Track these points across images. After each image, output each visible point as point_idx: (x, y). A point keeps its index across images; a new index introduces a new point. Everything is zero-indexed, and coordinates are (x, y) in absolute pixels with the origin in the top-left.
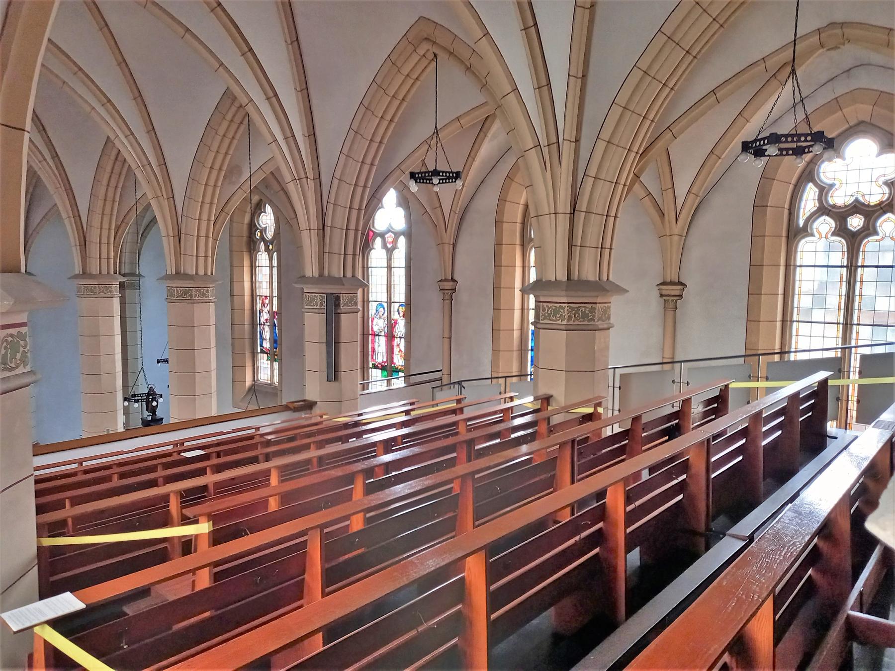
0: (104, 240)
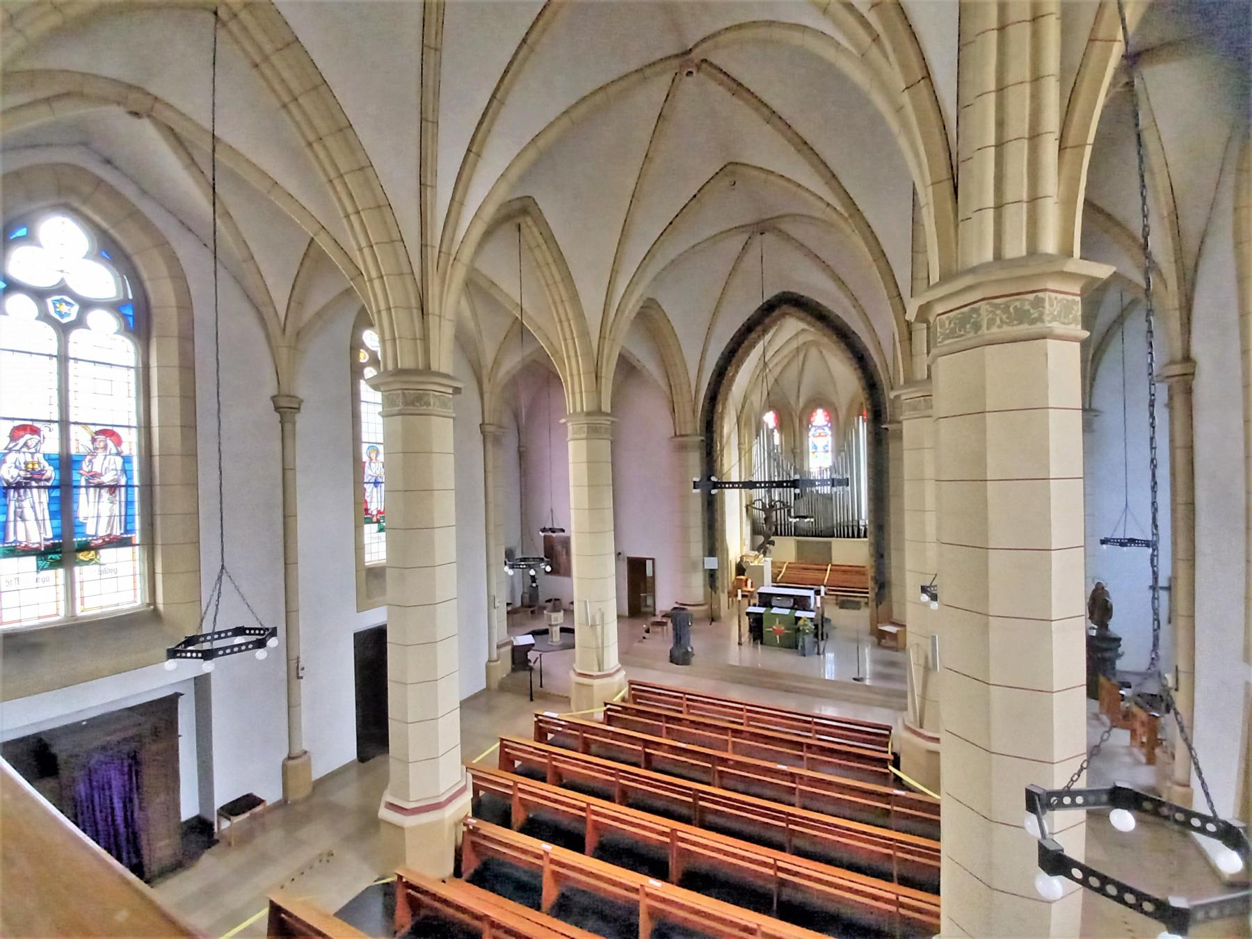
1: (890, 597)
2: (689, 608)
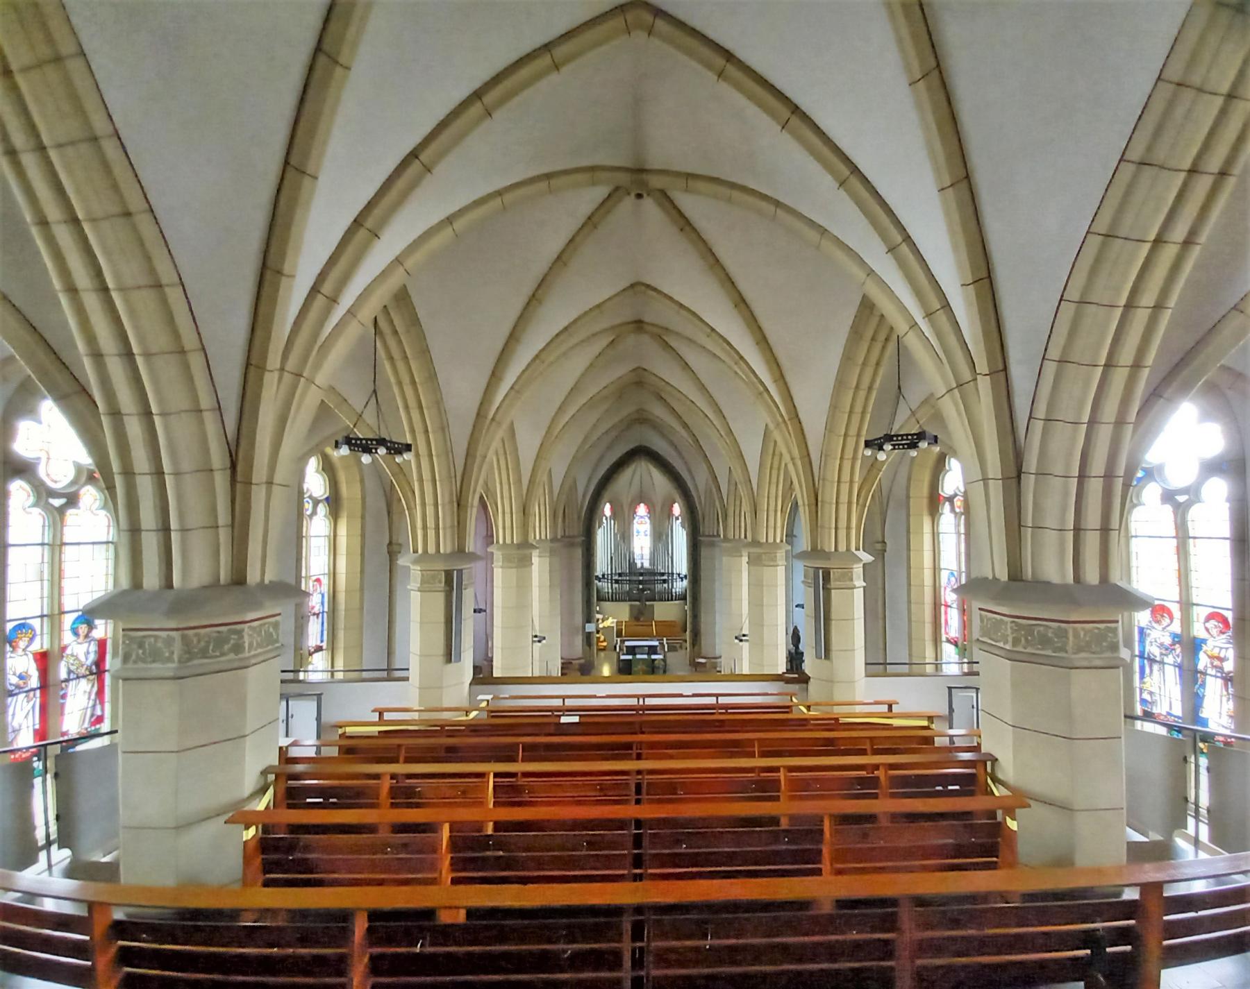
1: (700, 644)
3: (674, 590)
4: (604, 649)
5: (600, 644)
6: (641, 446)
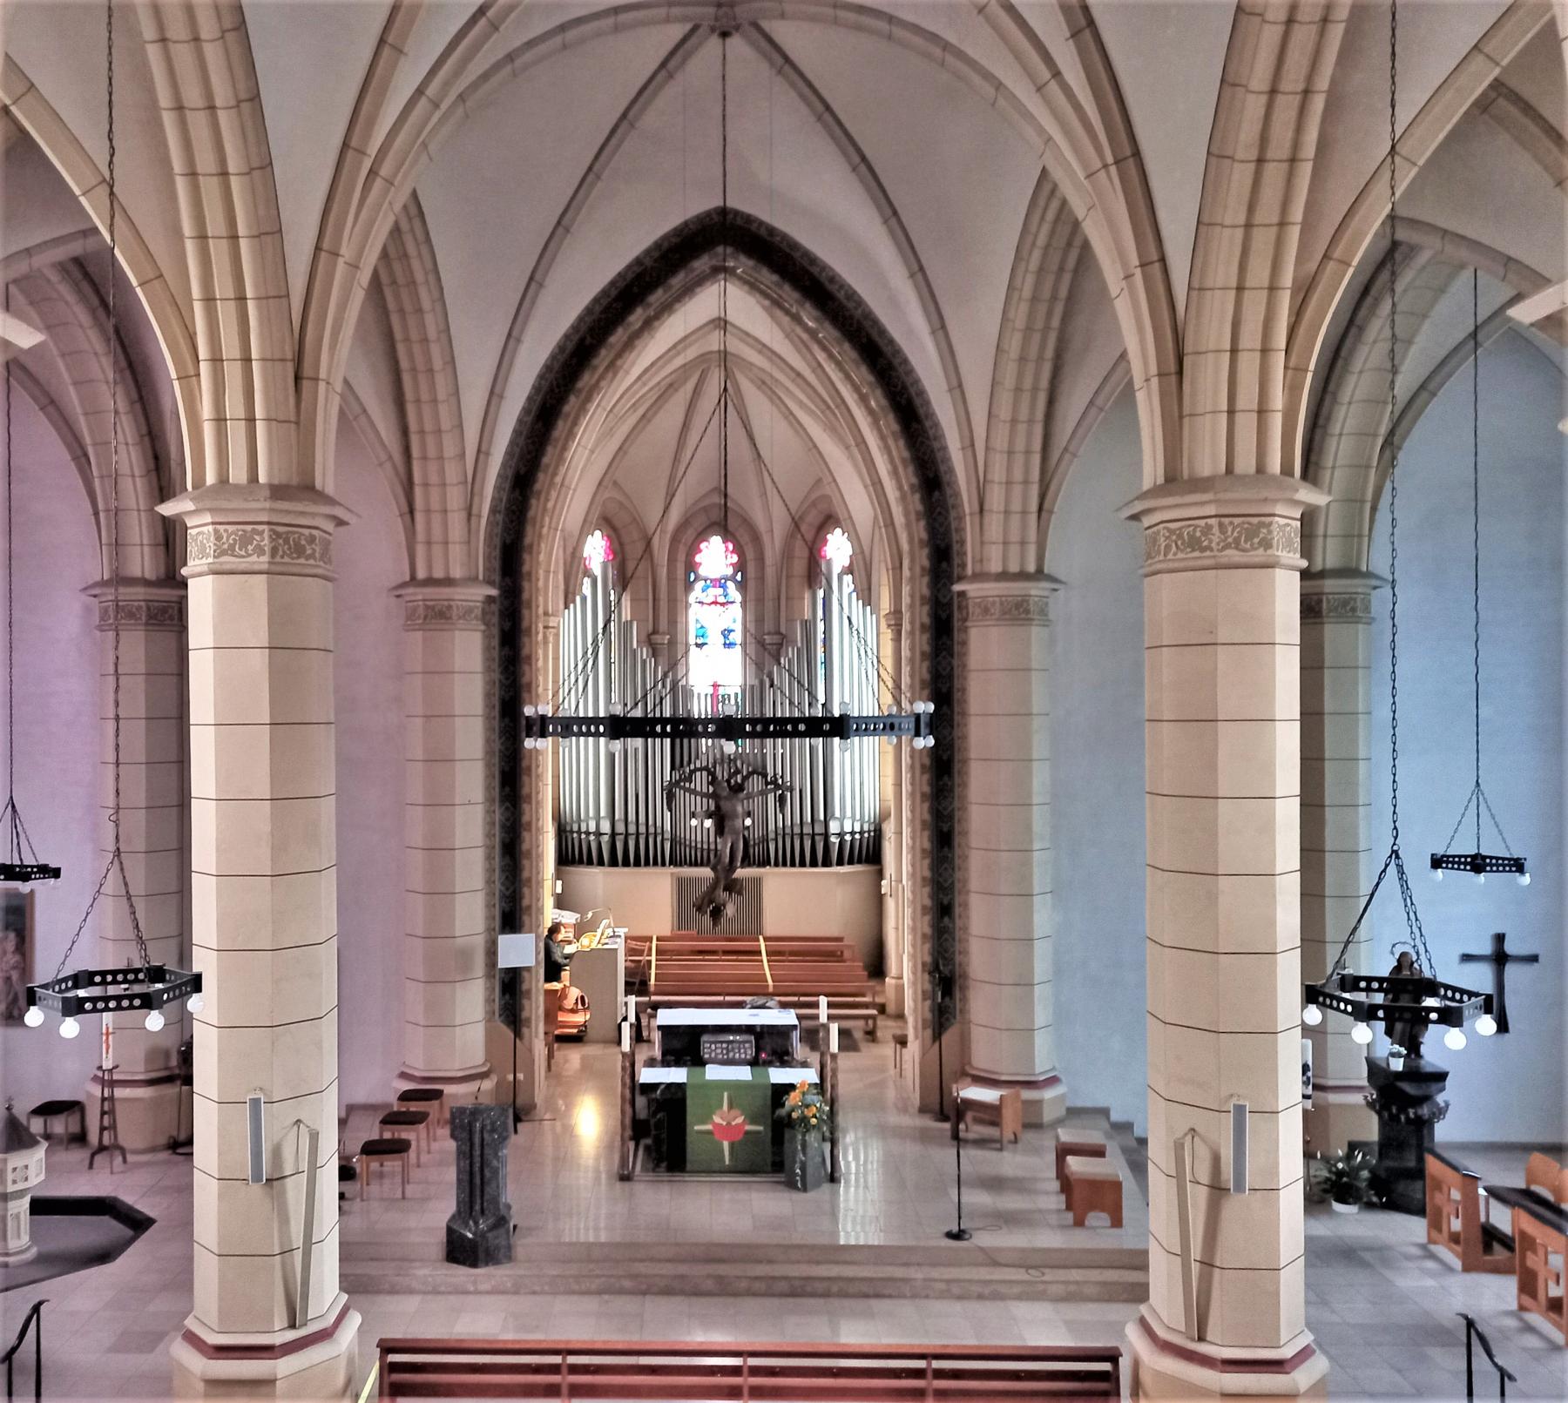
0: (1251, 337)
2: (449, 1089)
3: (834, 827)
4: (577, 1039)
5: (562, 1017)
6: (723, 211)
